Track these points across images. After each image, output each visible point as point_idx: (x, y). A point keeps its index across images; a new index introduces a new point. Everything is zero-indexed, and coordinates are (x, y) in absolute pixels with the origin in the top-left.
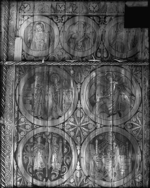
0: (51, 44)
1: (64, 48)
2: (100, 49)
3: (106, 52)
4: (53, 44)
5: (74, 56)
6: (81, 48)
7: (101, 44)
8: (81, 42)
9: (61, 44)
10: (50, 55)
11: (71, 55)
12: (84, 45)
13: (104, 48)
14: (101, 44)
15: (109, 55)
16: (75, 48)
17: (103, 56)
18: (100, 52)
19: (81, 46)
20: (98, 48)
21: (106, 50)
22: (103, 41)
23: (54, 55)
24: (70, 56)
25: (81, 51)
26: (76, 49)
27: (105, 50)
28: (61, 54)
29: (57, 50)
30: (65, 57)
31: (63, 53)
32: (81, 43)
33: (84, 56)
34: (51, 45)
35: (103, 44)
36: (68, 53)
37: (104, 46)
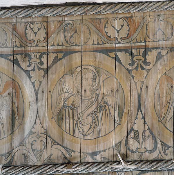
0: (16, 123)
1: (50, 133)
2: (136, 132)
3: (151, 138)
4: (22, 124)
5: (74, 151)
6: (90, 131)
7: (137, 118)
8: (88, 115)
9: (40, 124)
10: (16, 149)
11: (66, 148)
12: (95, 125)
13: (146, 128)
14: (137, 118)
15: (159, 146)
16: (74, 132)
17: (145, 148)
18: (136, 137)
19: (89, 126)
20: (132, 129)
21: (151, 133)
22: (143, 111)
23: (24, 151)
24: (64, 150)
25: (91, 138)
26: (77, 134)
27: (147, 133)
28: (43, 147)
29: (33, 139)
30: (51, 155)
31: (46, 146)
32: (90, 119)
33: (98, 150)
34: (16, 128)
35: (143, 118)
36: (58, 144)
37: (145, 123)
